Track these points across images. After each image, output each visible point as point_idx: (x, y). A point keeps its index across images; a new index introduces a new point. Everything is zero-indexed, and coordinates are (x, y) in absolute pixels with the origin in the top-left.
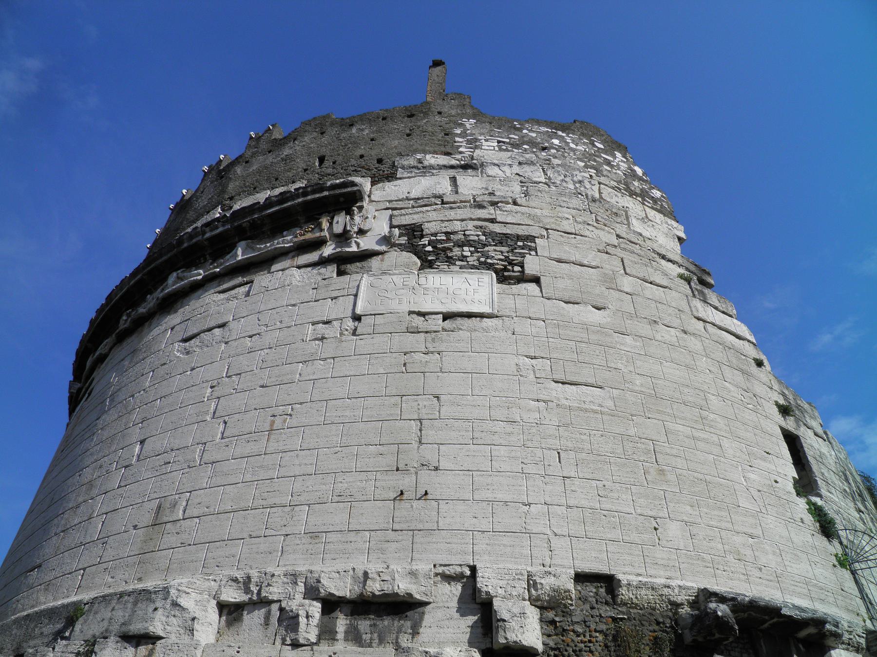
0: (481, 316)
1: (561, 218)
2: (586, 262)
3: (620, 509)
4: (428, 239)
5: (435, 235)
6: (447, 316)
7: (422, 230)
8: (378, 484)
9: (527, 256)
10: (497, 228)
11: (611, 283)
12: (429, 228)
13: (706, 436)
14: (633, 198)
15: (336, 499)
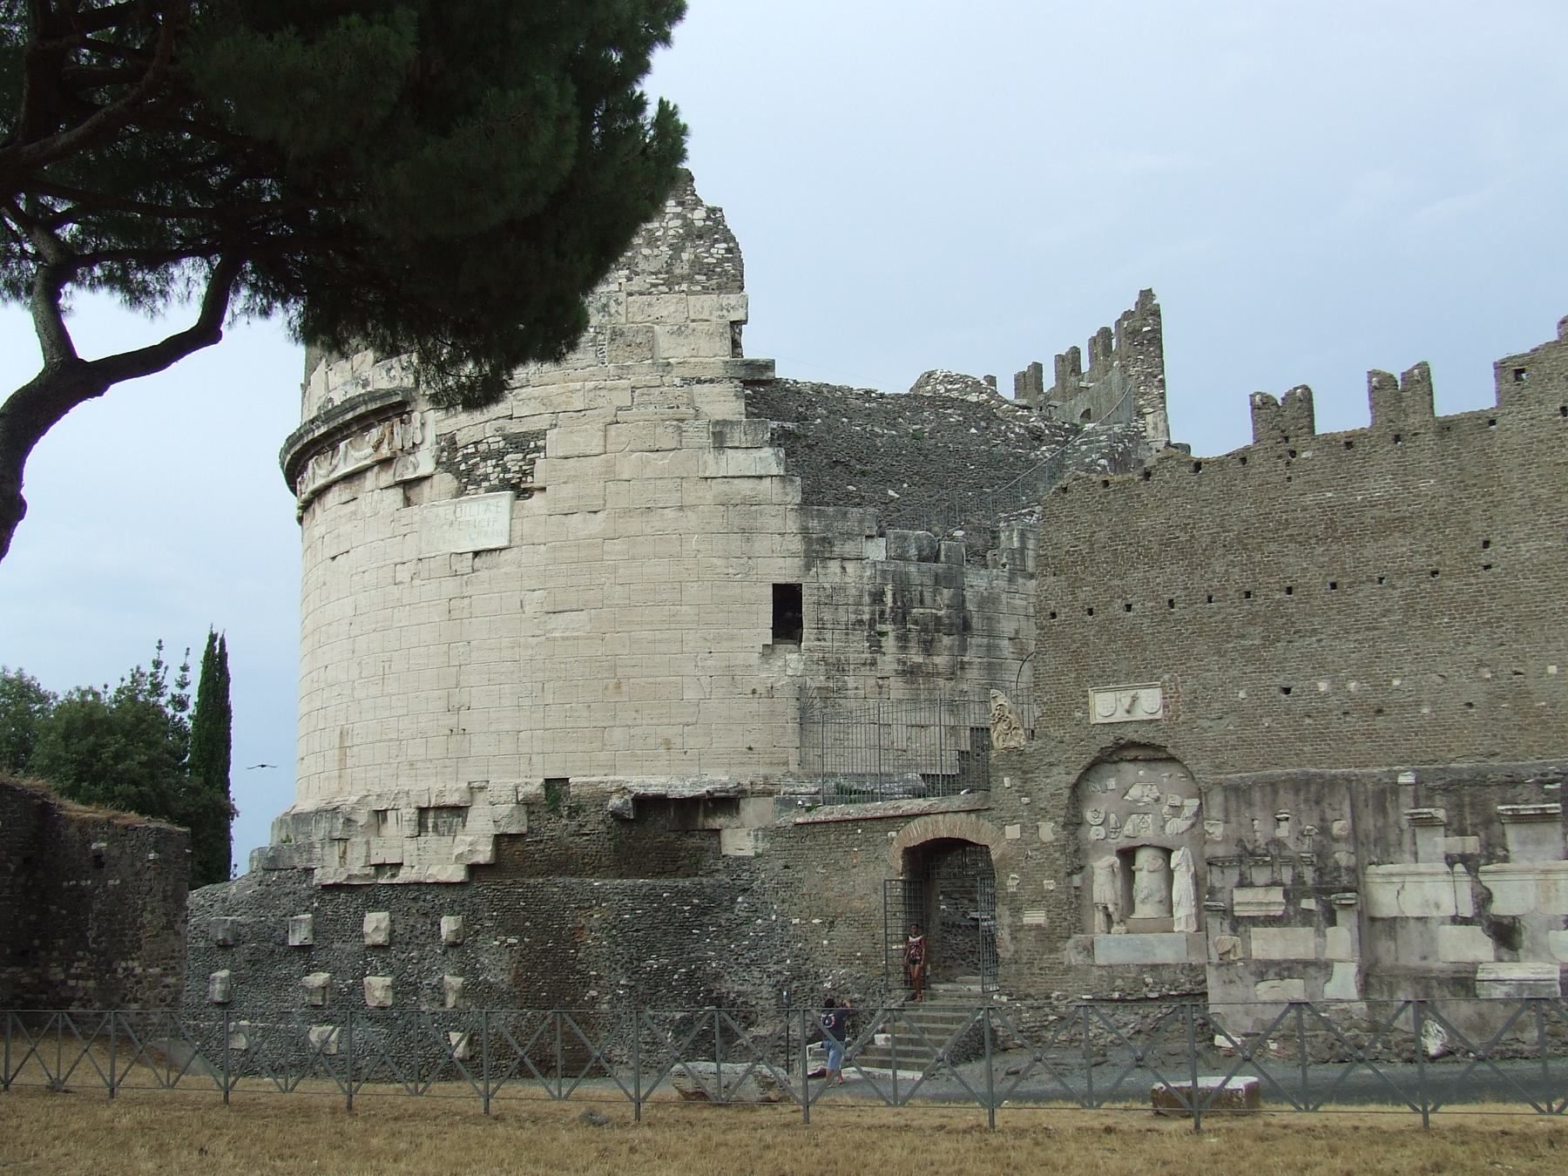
0: (501, 550)
1: (572, 392)
2: (588, 453)
3: (581, 725)
4: (461, 453)
5: (465, 447)
6: (476, 554)
7: (455, 443)
8: (440, 723)
9: (537, 461)
10: (514, 428)
11: (610, 476)
12: (461, 439)
13: (667, 636)
14: (675, 293)
15: (420, 735)
